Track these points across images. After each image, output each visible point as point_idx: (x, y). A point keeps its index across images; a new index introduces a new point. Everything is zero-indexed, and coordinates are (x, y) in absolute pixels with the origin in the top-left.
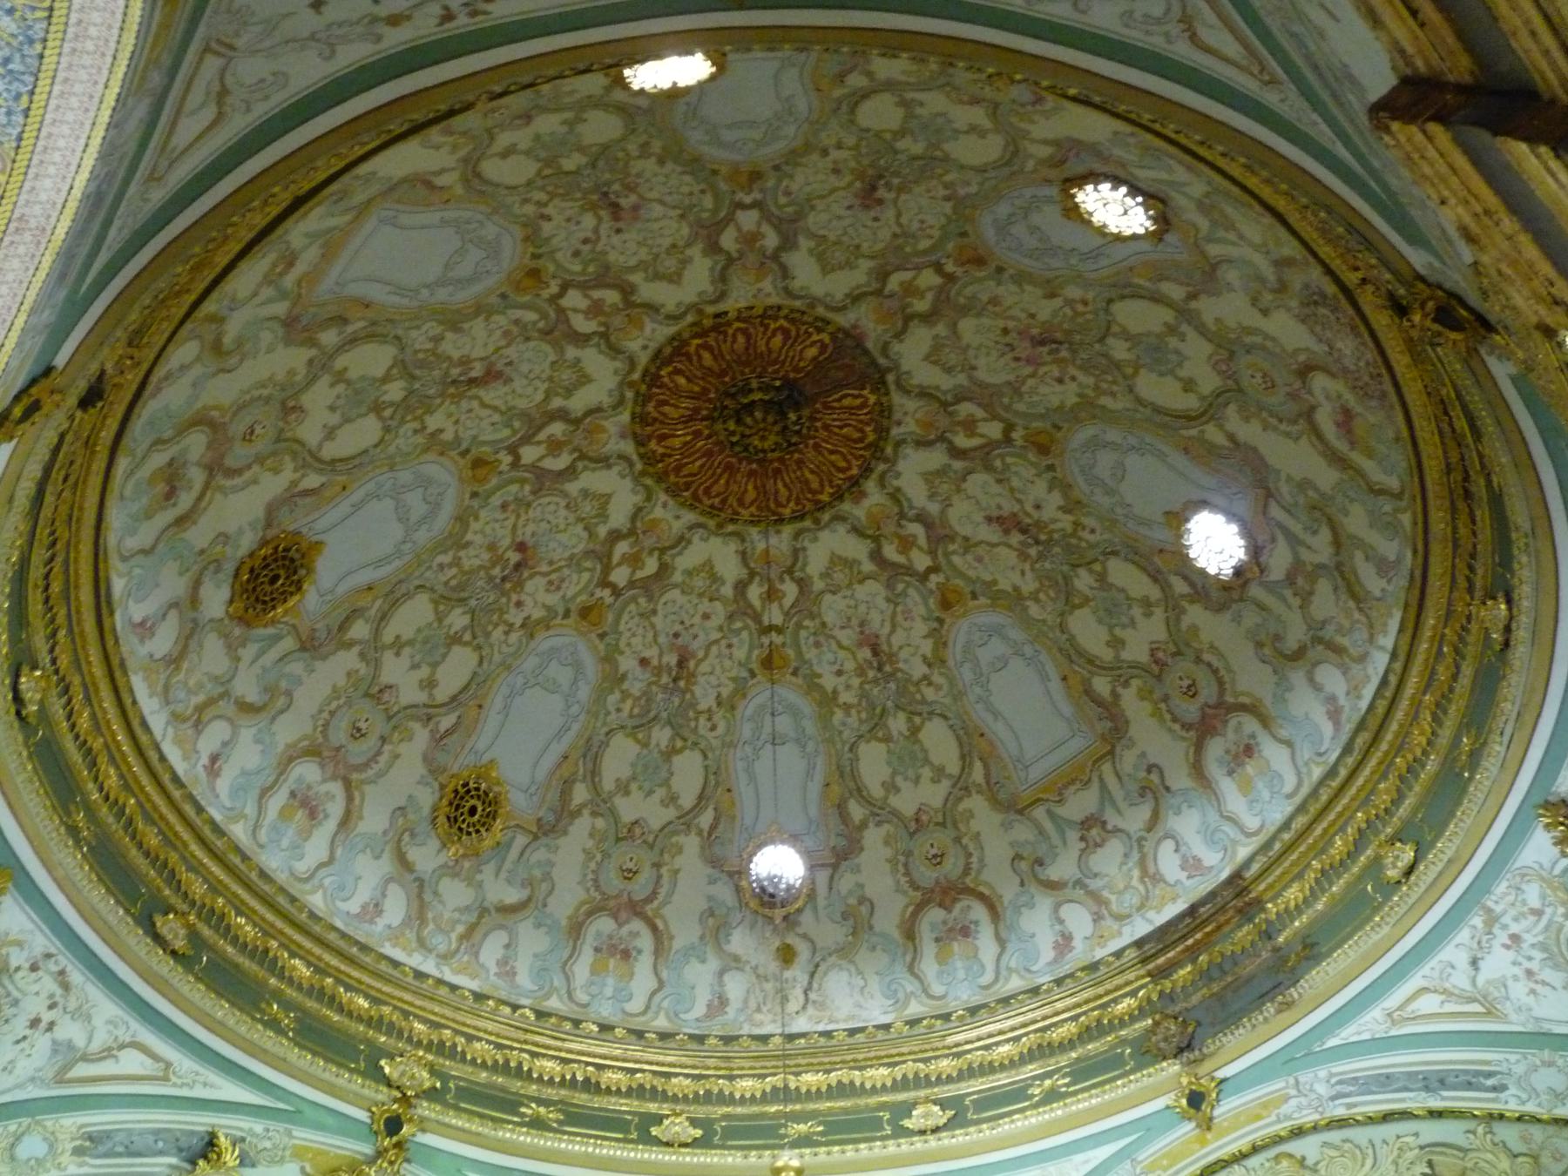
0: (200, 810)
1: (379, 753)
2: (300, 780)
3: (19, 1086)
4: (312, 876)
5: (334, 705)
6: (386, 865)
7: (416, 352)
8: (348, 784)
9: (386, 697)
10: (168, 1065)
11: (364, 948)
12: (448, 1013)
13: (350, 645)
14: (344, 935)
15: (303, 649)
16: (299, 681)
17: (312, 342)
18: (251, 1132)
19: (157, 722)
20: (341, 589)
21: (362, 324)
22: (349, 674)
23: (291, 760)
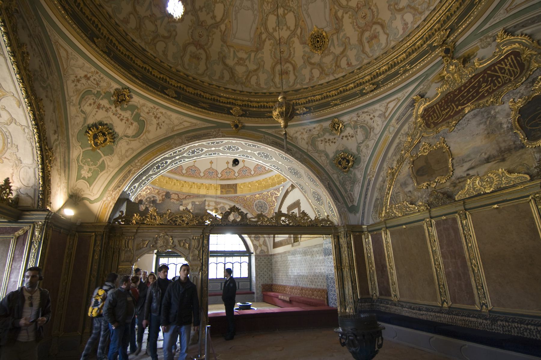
0: (353, 72)
1: (372, 10)
2: (366, 39)
3: (383, 125)
4: (387, 43)
5: (355, 24)
6: (399, 17)
7: (271, 8)
8: (375, 23)
9: (359, 6)
10: (397, 98)
11: (409, 36)
12: (438, 15)
13: (343, 17)
14: (402, 41)
15: (338, 32)
16: (345, 34)
17: (265, 41)
18: (421, 89)
19: (332, 78)
20: (328, 19)
21: (262, 28)
22: (350, 18)
23: (361, 40)
